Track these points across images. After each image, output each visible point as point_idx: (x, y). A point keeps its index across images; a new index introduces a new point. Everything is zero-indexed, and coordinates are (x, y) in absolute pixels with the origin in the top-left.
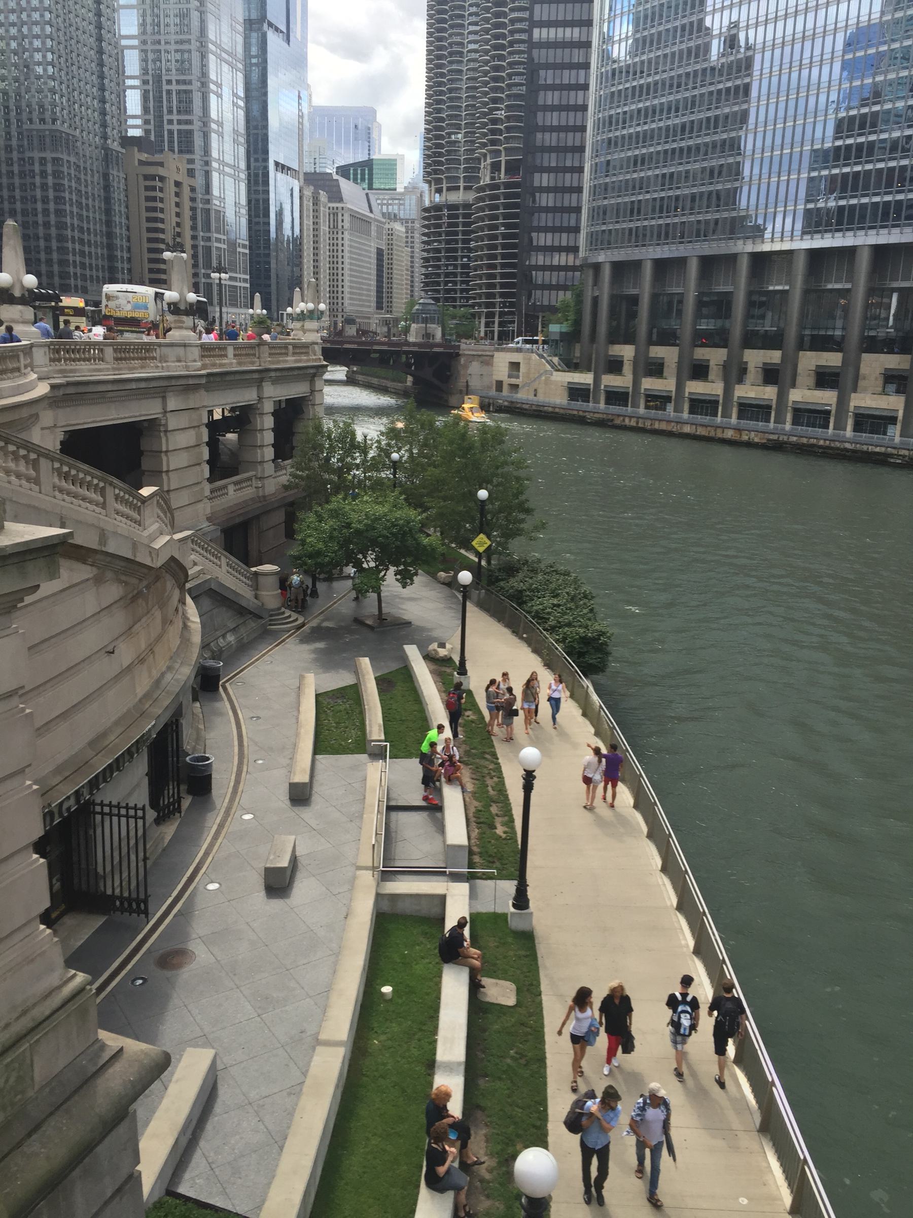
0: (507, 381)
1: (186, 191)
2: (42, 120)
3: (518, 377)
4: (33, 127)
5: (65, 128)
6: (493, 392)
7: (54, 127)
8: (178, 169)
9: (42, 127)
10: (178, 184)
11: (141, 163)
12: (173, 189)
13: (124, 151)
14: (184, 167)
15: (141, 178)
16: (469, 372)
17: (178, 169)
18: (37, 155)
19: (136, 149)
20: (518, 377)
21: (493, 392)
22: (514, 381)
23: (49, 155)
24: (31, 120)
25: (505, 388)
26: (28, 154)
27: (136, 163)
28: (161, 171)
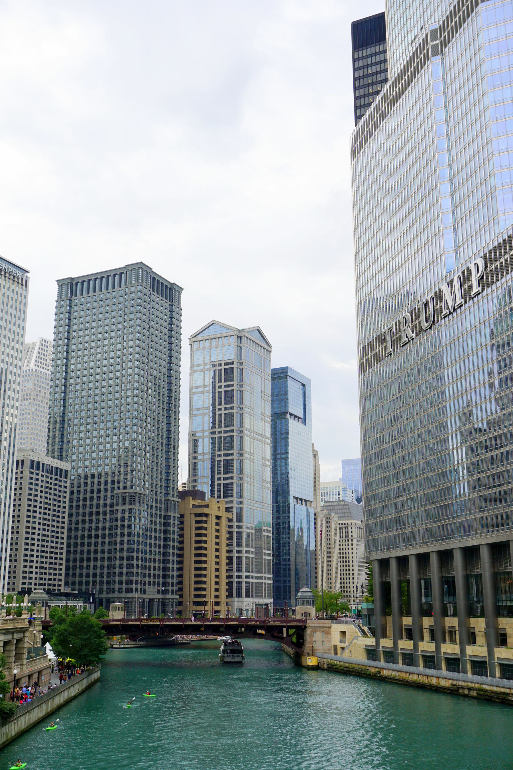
0: (340, 645)
1: (224, 523)
2: (125, 488)
3: (345, 643)
4: (120, 491)
5: (138, 490)
6: (332, 655)
7: (131, 491)
8: (219, 508)
9: (125, 491)
10: (218, 518)
11: (194, 506)
12: (215, 521)
13: (180, 500)
14: (223, 506)
15: (193, 516)
16: (314, 639)
17: (219, 508)
18: (120, 508)
19: (191, 498)
20: (345, 643)
21: (332, 655)
22: (343, 645)
23: (127, 507)
24: (119, 488)
25: (339, 651)
26: (115, 508)
27: (191, 507)
28: (206, 511)
